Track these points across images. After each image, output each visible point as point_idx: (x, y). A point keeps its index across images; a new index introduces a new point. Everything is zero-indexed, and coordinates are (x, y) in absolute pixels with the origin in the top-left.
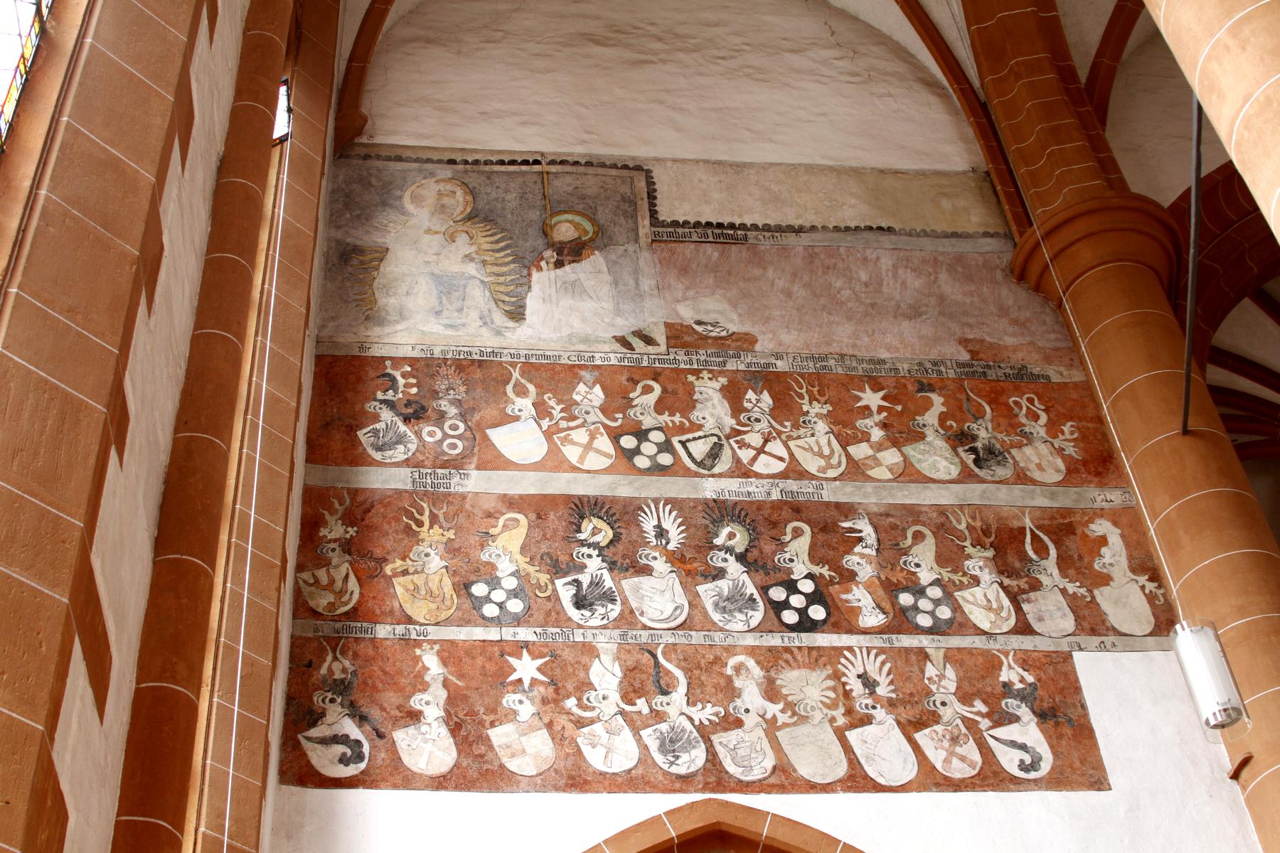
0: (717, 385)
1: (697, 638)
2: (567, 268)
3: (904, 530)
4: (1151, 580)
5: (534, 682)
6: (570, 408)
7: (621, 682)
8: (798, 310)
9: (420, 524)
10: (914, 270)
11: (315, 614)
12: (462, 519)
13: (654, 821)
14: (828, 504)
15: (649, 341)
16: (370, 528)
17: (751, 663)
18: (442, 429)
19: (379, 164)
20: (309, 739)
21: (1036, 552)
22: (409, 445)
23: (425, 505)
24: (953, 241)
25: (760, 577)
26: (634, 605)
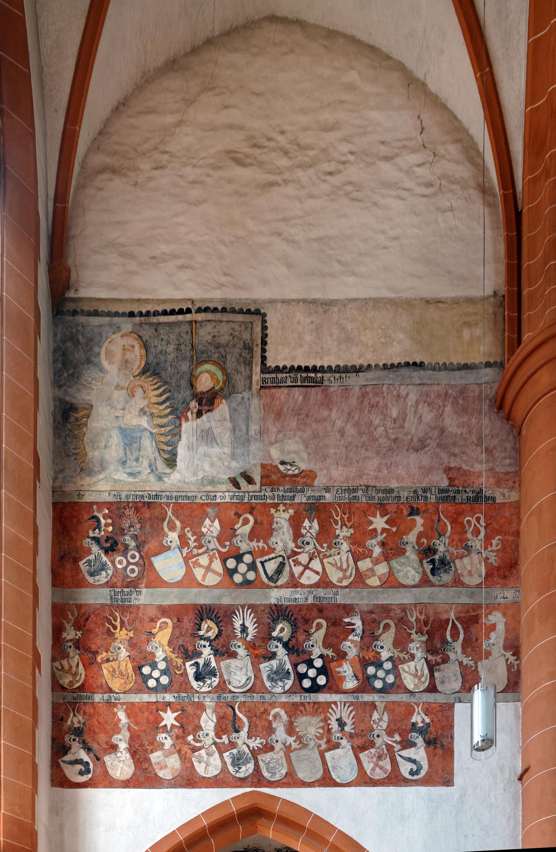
0: (287, 516)
1: (256, 697)
2: (204, 417)
3: (379, 623)
4: (513, 655)
5: (173, 725)
6: (200, 536)
7: (216, 725)
8: (346, 447)
9: (115, 628)
10: (429, 405)
11: (63, 688)
12: (137, 624)
13: (226, 803)
14: (339, 606)
15: (250, 480)
16: (90, 631)
17: (283, 713)
18: (126, 558)
19: (82, 319)
20: (64, 762)
21: (452, 636)
22: (109, 572)
23: (117, 614)
24: (463, 373)
25: (294, 657)
26: (226, 677)
